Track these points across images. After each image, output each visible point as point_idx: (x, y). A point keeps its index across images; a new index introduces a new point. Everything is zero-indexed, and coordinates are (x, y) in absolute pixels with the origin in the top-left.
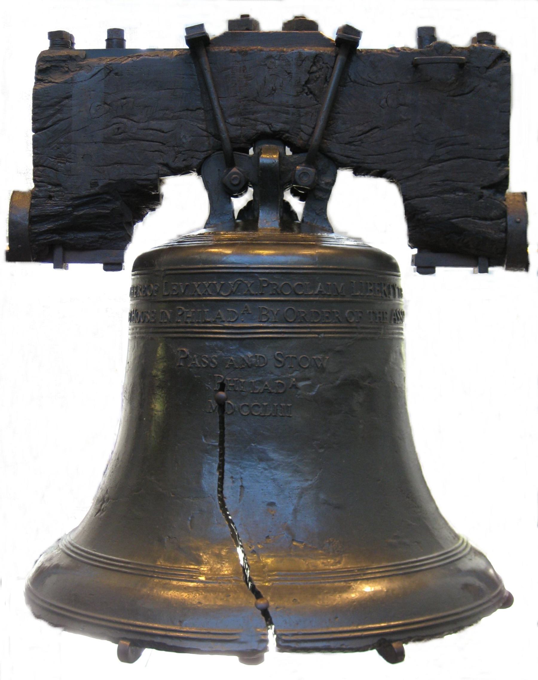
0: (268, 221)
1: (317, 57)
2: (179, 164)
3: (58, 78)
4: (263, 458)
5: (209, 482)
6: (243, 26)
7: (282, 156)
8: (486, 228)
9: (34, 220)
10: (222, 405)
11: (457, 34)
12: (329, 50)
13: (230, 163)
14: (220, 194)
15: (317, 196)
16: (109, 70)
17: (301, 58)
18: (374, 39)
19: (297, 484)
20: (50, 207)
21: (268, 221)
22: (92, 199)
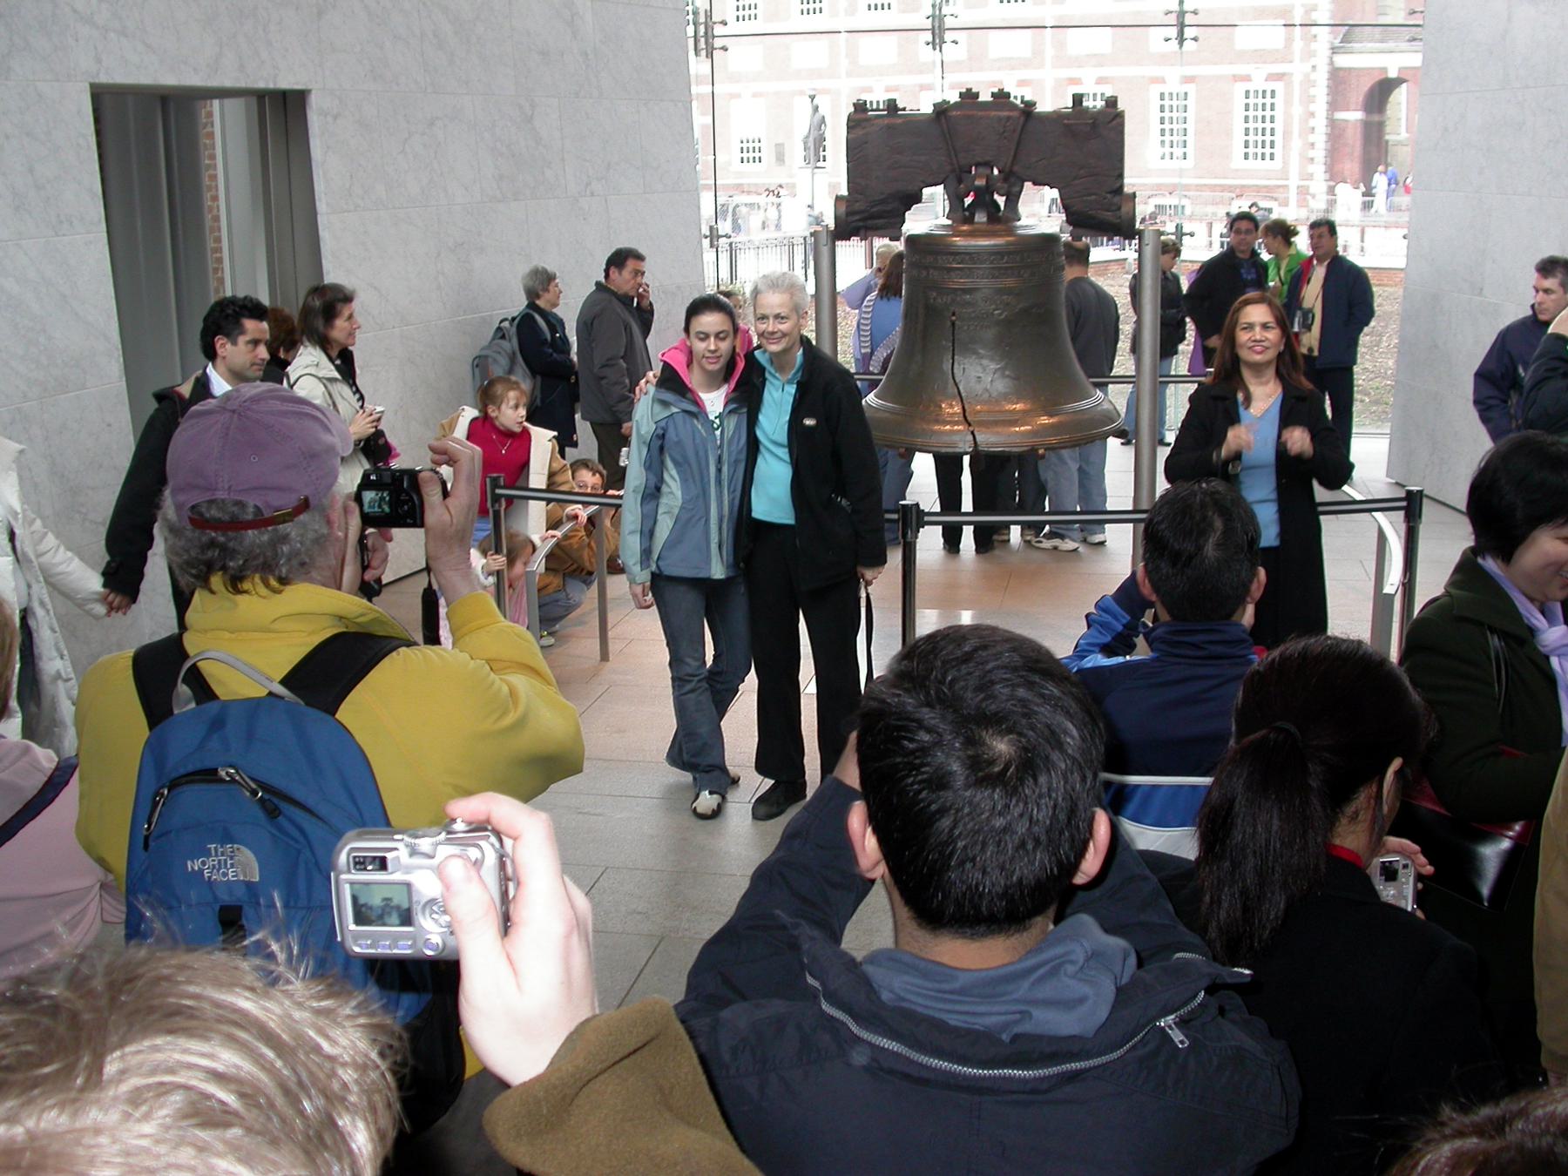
0: (981, 217)
1: (1009, 118)
2: (930, 181)
3: (859, 132)
4: (975, 353)
5: (947, 366)
6: (969, 96)
7: (989, 178)
8: (1108, 216)
9: (848, 214)
10: (953, 324)
11: (1094, 104)
12: (1015, 114)
13: (960, 181)
14: (955, 199)
15: (1013, 200)
16: (889, 127)
17: (1000, 119)
18: (1045, 106)
19: (993, 366)
20: (857, 206)
21: (981, 217)
22: (882, 202)
